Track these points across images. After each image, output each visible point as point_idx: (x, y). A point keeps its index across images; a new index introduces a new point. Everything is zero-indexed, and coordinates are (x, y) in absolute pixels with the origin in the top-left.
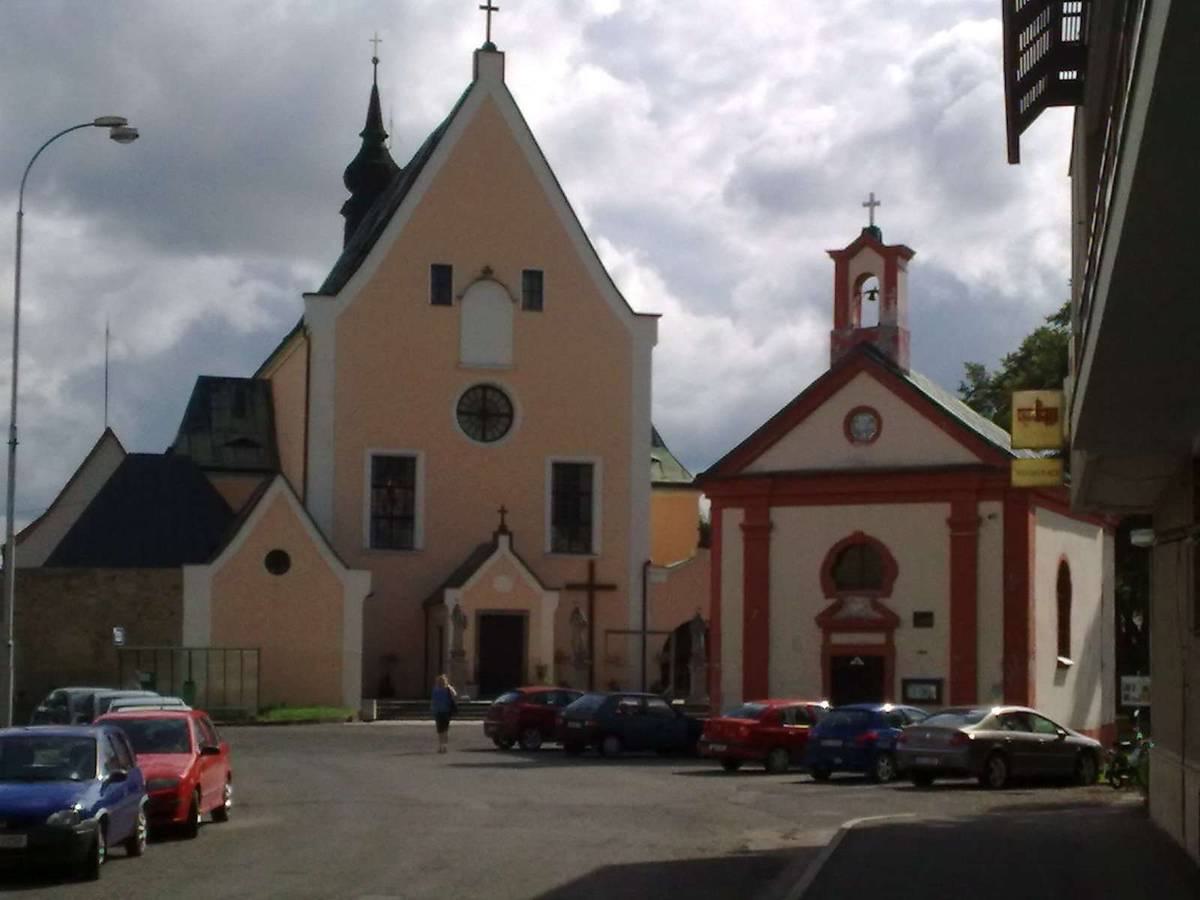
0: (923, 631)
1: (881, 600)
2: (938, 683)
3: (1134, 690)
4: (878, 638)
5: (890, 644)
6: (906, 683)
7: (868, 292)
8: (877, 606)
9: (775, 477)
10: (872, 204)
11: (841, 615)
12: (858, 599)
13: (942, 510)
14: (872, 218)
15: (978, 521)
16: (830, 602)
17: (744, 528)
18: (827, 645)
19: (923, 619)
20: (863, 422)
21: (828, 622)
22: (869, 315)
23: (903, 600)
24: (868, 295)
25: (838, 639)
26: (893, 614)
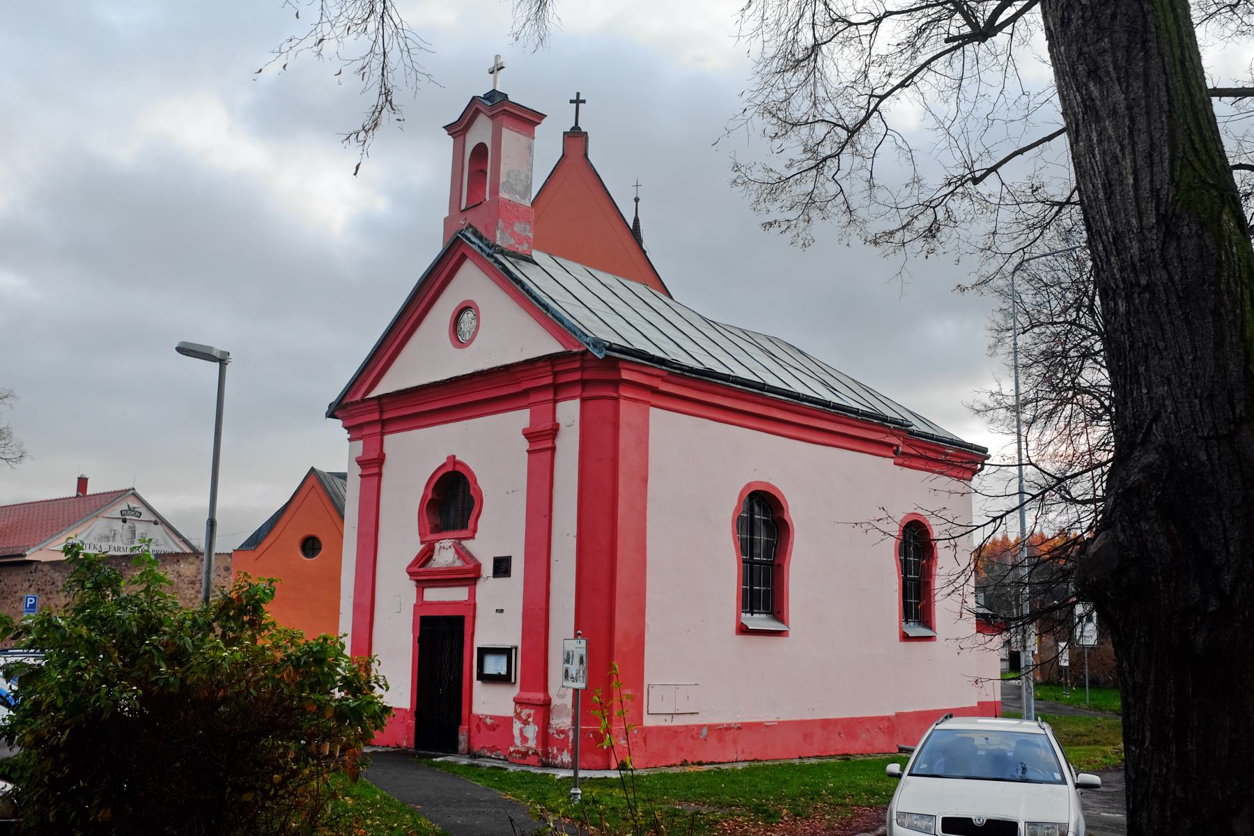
0: (502, 581)
1: (467, 544)
2: (507, 652)
4: (458, 594)
5: (471, 605)
6: (483, 652)
13: (521, 419)
15: (554, 431)
18: (420, 604)
23: (483, 548)
25: (432, 595)
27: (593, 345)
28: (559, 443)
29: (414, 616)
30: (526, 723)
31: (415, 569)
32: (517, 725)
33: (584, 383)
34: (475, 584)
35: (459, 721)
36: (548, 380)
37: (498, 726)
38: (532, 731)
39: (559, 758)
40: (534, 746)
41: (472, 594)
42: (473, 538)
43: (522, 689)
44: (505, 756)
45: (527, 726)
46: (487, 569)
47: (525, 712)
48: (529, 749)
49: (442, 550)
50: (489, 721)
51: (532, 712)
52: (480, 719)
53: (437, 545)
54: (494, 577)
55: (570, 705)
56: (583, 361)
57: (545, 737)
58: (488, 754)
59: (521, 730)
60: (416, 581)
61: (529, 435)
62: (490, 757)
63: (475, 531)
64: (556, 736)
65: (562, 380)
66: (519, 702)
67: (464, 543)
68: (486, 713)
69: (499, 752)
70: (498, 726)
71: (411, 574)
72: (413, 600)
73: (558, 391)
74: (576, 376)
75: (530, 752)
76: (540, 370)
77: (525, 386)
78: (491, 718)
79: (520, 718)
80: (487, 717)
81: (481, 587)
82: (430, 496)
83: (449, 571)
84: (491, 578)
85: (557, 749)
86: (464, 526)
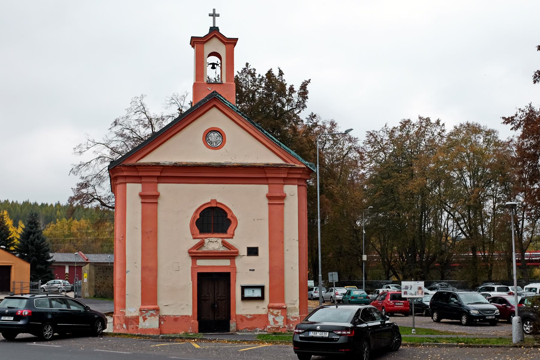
0: (253, 258)
2: (262, 288)
3: (411, 289)
4: (226, 263)
6: (243, 288)
7: (210, 64)
8: (225, 244)
9: (157, 166)
10: (214, 15)
11: (204, 249)
13: (264, 189)
15: (283, 197)
16: (197, 241)
17: (142, 196)
19: (253, 252)
20: (214, 137)
21: (195, 255)
24: (211, 66)
25: (200, 262)
27: (310, 165)
28: (286, 202)
29: (192, 272)
30: (276, 316)
31: (195, 251)
32: (271, 318)
33: (299, 179)
34: (235, 259)
35: (229, 318)
36: (285, 176)
38: (280, 320)
41: (233, 263)
42: (232, 238)
43: (270, 302)
45: (277, 317)
46: (243, 251)
47: (275, 312)
48: (280, 326)
49: (210, 242)
50: (249, 317)
51: (280, 311)
52: (243, 316)
53: (206, 241)
54: (247, 256)
55: (298, 307)
56: (303, 171)
57: (287, 321)
58: (249, 330)
59: (274, 319)
60: (192, 256)
61: (269, 198)
63: (233, 235)
64: (292, 320)
65: (291, 176)
66: (269, 308)
67: (225, 240)
68: (247, 313)
71: (190, 253)
72: (190, 265)
73: (287, 180)
74: (299, 176)
75: (281, 327)
76: (283, 171)
77: (268, 175)
78: (250, 315)
79: (272, 314)
80: (247, 315)
81: (238, 262)
82: (198, 217)
85: (293, 325)
86: (225, 232)
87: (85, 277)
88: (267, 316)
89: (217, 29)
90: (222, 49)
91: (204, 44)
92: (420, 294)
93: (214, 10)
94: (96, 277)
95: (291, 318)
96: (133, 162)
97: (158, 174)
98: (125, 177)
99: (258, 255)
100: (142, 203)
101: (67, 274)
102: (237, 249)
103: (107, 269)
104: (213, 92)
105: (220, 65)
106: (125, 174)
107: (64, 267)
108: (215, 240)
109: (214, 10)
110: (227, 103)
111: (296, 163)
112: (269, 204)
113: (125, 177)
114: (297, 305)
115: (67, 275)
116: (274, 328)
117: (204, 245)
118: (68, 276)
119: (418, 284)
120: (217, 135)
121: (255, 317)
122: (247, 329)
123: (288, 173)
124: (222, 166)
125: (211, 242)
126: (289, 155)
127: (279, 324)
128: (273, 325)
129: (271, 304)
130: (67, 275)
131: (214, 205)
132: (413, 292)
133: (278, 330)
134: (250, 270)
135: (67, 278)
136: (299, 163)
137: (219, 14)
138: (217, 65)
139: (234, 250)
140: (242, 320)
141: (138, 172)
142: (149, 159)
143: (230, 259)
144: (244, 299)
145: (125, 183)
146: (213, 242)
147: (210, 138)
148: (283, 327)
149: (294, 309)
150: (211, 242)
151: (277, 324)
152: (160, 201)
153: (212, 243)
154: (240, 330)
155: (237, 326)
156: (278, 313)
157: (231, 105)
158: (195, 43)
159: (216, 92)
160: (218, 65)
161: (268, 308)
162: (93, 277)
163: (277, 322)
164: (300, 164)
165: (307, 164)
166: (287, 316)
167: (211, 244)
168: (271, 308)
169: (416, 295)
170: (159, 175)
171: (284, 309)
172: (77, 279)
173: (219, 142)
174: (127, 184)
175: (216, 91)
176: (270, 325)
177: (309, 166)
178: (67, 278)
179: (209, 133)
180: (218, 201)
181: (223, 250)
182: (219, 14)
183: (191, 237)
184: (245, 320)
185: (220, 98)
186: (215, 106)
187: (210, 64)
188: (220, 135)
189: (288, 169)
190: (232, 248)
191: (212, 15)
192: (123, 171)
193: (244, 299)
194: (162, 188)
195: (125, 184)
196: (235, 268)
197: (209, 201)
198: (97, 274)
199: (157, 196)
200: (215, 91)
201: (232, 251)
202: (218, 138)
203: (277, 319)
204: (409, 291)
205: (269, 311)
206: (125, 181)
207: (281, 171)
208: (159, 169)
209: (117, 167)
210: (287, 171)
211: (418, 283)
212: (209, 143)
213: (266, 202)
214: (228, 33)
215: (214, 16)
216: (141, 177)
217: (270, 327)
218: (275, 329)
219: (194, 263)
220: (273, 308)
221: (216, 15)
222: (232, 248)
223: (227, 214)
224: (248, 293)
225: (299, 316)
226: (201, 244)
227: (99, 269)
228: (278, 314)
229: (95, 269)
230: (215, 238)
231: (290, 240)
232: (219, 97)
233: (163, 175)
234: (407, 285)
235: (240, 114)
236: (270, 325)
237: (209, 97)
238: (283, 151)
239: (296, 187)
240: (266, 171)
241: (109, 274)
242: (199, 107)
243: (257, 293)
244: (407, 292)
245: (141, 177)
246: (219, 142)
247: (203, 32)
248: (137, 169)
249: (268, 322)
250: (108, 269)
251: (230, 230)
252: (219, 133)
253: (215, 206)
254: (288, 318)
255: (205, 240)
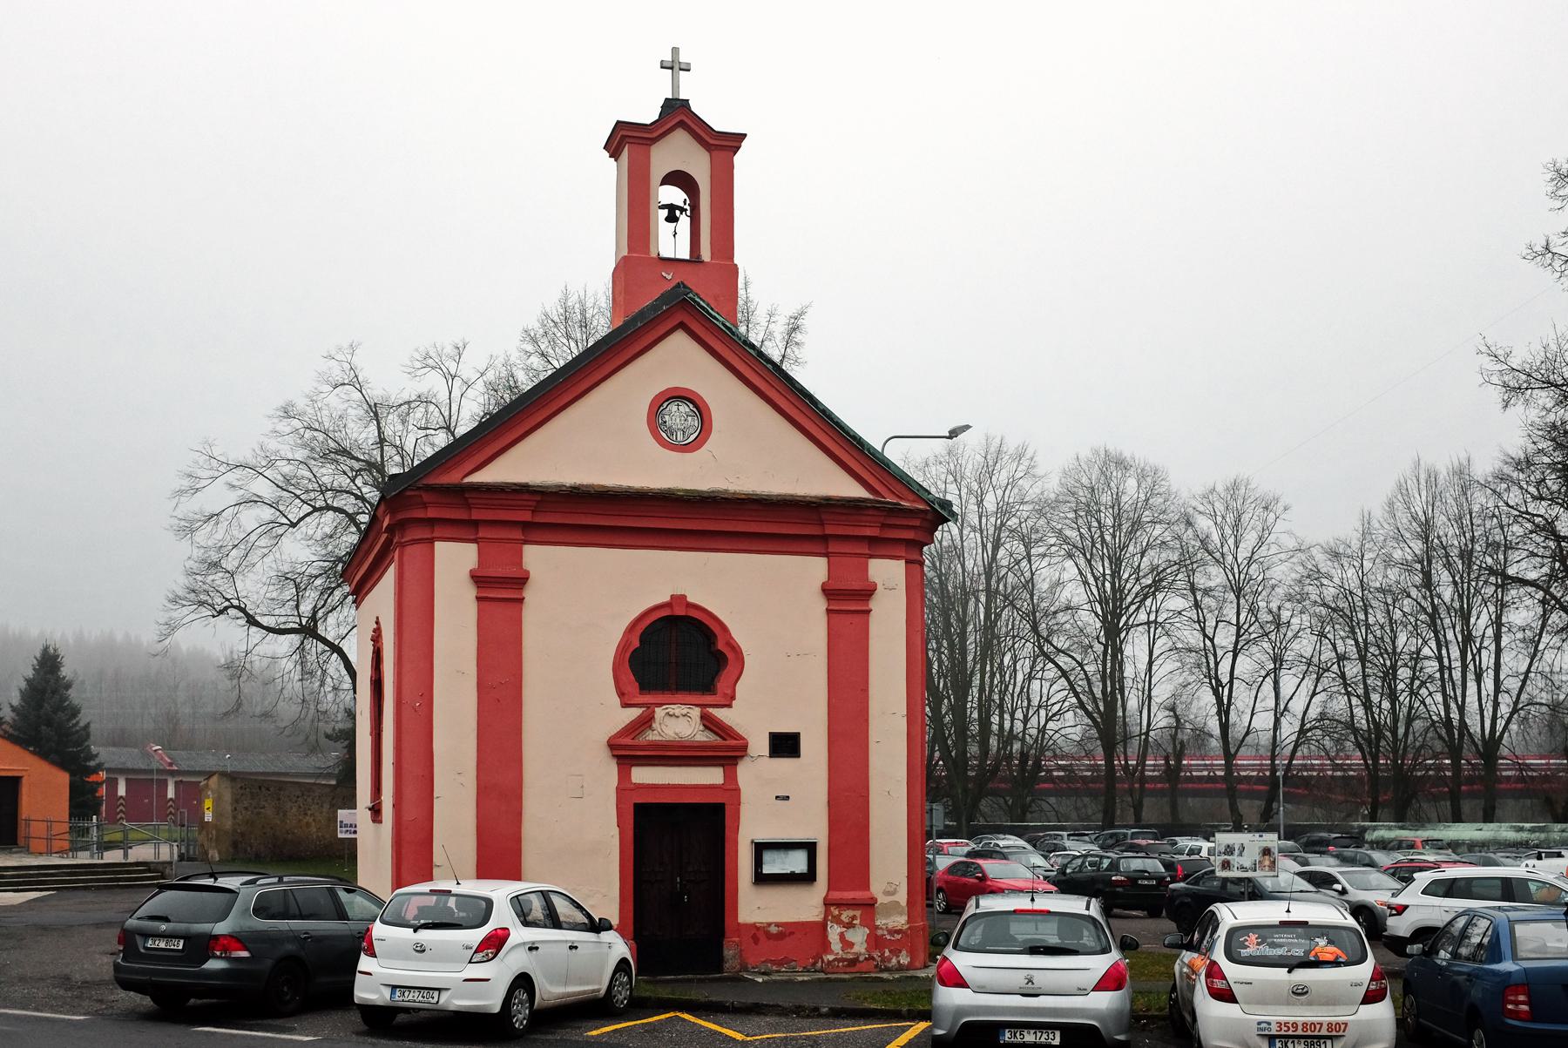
2: (810, 848)
3: (1241, 855)
4: (711, 776)
5: (731, 788)
6: (760, 848)
7: (663, 207)
8: (709, 723)
10: (675, 66)
11: (651, 737)
12: (677, 710)
13: (815, 569)
14: (675, 85)
15: (868, 592)
16: (634, 713)
17: (478, 579)
18: (625, 788)
19: (785, 745)
20: (678, 415)
22: (672, 241)
24: (665, 213)
25: (642, 775)
26: (737, 737)
30: (850, 925)
31: (627, 741)
32: (834, 932)
34: (736, 764)
37: (792, 933)
38: (858, 937)
39: (894, 961)
40: (863, 951)
41: (731, 777)
42: (729, 706)
43: (830, 888)
44: (804, 968)
45: (851, 930)
46: (759, 745)
47: (846, 915)
49: (667, 718)
50: (774, 930)
51: (858, 913)
54: (770, 757)
55: (903, 902)
57: (875, 941)
58: (774, 968)
59: (842, 936)
61: (828, 592)
62: (779, 972)
63: (733, 697)
64: (888, 937)
66: (828, 903)
67: (711, 710)
68: (770, 920)
69: (793, 963)
70: (792, 933)
71: (613, 745)
72: (613, 780)
73: (880, 546)
75: (861, 959)
76: (869, 518)
77: (829, 530)
78: (777, 925)
79: (838, 920)
80: (769, 924)
81: (744, 771)
82: (636, 643)
83: (698, 747)
84: (768, 759)
86: (708, 687)
87: (206, 807)
88: (822, 926)
89: (685, 104)
90: (699, 165)
91: (651, 145)
92: (1267, 868)
93: (675, 51)
94: (235, 809)
95: (886, 933)
96: (451, 478)
97: (526, 516)
98: (432, 522)
99: (799, 756)
100: (479, 599)
101: (121, 797)
102: (743, 738)
103: (260, 788)
104: (678, 285)
105: (688, 213)
106: (432, 513)
107: (165, 783)
108: (685, 712)
109: (675, 51)
110: (717, 320)
111: (901, 498)
112: (829, 611)
113: (432, 522)
114: (902, 897)
115: (121, 801)
116: (843, 960)
117: (654, 725)
118: (124, 802)
119: (1261, 839)
120: (687, 410)
121: (789, 931)
122: (769, 965)
123: (883, 526)
124: (707, 498)
125: (671, 716)
126: (885, 475)
127: (856, 949)
128: (841, 952)
129: (836, 895)
130: (121, 801)
131: (680, 611)
132: (1247, 863)
133: (855, 965)
134: (777, 797)
135: (121, 808)
136: (911, 497)
137: (689, 64)
138: (682, 210)
139: (736, 739)
140: (756, 939)
141: (469, 507)
142: (493, 474)
143: (723, 765)
144: (761, 879)
145: (431, 541)
146: (678, 717)
147: (667, 417)
148: (866, 959)
149: (893, 908)
150: (671, 716)
151: (849, 950)
152: (530, 594)
153: (673, 719)
154: (750, 966)
155: (741, 956)
156: (854, 918)
157: (728, 324)
158: (627, 140)
159: (685, 286)
160: (686, 210)
161: (825, 904)
162: (229, 808)
163: (851, 945)
164: (914, 501)
165: (932, 502)
166: (877, 928)
167: (670, 721)
168: (833, 905)
169: (1255, 870)
170: (530, 520)
171: (869, 906)
172: (184, 813)
173: (691, 431)
174: (437, 544)
175: (685, 282)
176: (831, 952)
177: (937, 507)
178: (121, 808)
179: (665, 405)
180: (691, 599)
181: (705, 739)
182: (689, 64)
183: (617, 700)
184: (762, 938)
185: (699, 304)
186: (682, 326)
187: (663, 207)
188: (695, 410)
189: (885, 513)
190: (730, 736)
191: (670, 65)
192: (425, 506)
193: (761, 879)
194: (538, 558)
195: (429, 544)
196: (737, 790)
197: (667, 599)
198: (237, 801)
199: (521, 581)
200: (682, 283)
201: (734, 742)
202: (690, 418)
203: (851, 936)
204: (1235, 859)
205: (827, 913)
206: (429, 536)
207: (864, 518)
208: (530, 503)
209: (408, 493)
210: (882, 519)
211: (1261, 836)
212: (665, 431)
213: (821, 605)
214: (719, 122)
215: (676, 67)
216: (475, 524)
217: (831, 957)
218: (845, 963)
219: (624, 775)
220: (841, 905)
221: (682, 67)
222: (730, 736)
223: (716, 636)
224: (775, 864)
225: (907, 926)
226: (646, 722)
227: (241, 788)
228: (854, 922)
229: (232, 788)
230: (683, 707)
231: (883, 713)
232: (695, 302)
233: (540, 519)
234: (1230, 842)
235: (751, 351)
236: (831, 952)
237: (664, 298)
238: (870, 462)
239: (902, 563)
240: (823, 516)
241: (266, 801)
242: (639, 325)
243: (796, 862)
244: (1232, 862)
245: (475, 524)
246: (691, 431)
247: (648, 114)
248: (466, 499)
249: (826, 946)
250: (263, 789)
251: (722, 684)
252: (691, 406)
253: (684, 614)
254: (879, 932)
255: (656, 709)
